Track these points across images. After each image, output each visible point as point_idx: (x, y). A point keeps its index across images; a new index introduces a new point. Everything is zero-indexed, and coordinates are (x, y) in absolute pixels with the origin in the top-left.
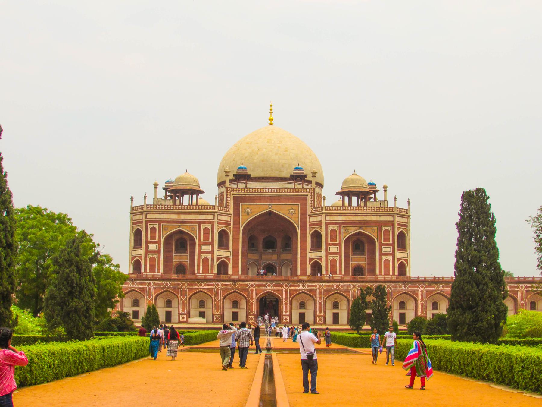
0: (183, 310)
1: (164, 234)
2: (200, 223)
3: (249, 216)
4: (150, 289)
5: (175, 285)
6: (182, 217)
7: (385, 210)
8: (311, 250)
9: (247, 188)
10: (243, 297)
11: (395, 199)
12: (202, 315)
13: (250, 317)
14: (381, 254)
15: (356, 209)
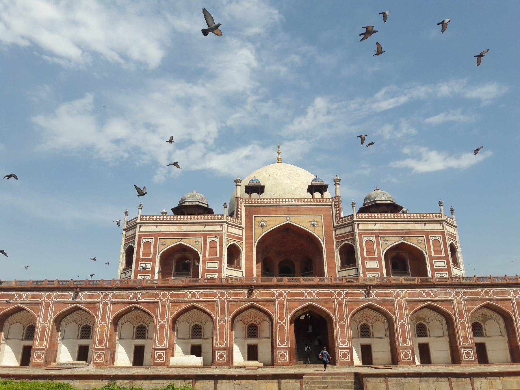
0: (161, 343)
1: (160, 249)
2: (205, 235)
3: (264, 230)
4: (105, 304)
5: (149, 296)
6: (184, 228)
7: (429, 216)
8: (341, 268)
9: (261, 199)
10: (266, 318)
11: (440, 203)
12: (196, 351)
13: (279, 353)
14: (433, 270)
15: (394, 216)
